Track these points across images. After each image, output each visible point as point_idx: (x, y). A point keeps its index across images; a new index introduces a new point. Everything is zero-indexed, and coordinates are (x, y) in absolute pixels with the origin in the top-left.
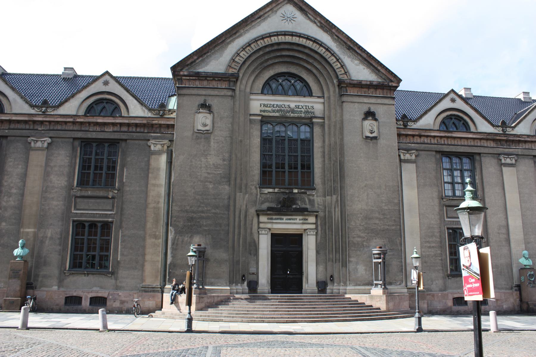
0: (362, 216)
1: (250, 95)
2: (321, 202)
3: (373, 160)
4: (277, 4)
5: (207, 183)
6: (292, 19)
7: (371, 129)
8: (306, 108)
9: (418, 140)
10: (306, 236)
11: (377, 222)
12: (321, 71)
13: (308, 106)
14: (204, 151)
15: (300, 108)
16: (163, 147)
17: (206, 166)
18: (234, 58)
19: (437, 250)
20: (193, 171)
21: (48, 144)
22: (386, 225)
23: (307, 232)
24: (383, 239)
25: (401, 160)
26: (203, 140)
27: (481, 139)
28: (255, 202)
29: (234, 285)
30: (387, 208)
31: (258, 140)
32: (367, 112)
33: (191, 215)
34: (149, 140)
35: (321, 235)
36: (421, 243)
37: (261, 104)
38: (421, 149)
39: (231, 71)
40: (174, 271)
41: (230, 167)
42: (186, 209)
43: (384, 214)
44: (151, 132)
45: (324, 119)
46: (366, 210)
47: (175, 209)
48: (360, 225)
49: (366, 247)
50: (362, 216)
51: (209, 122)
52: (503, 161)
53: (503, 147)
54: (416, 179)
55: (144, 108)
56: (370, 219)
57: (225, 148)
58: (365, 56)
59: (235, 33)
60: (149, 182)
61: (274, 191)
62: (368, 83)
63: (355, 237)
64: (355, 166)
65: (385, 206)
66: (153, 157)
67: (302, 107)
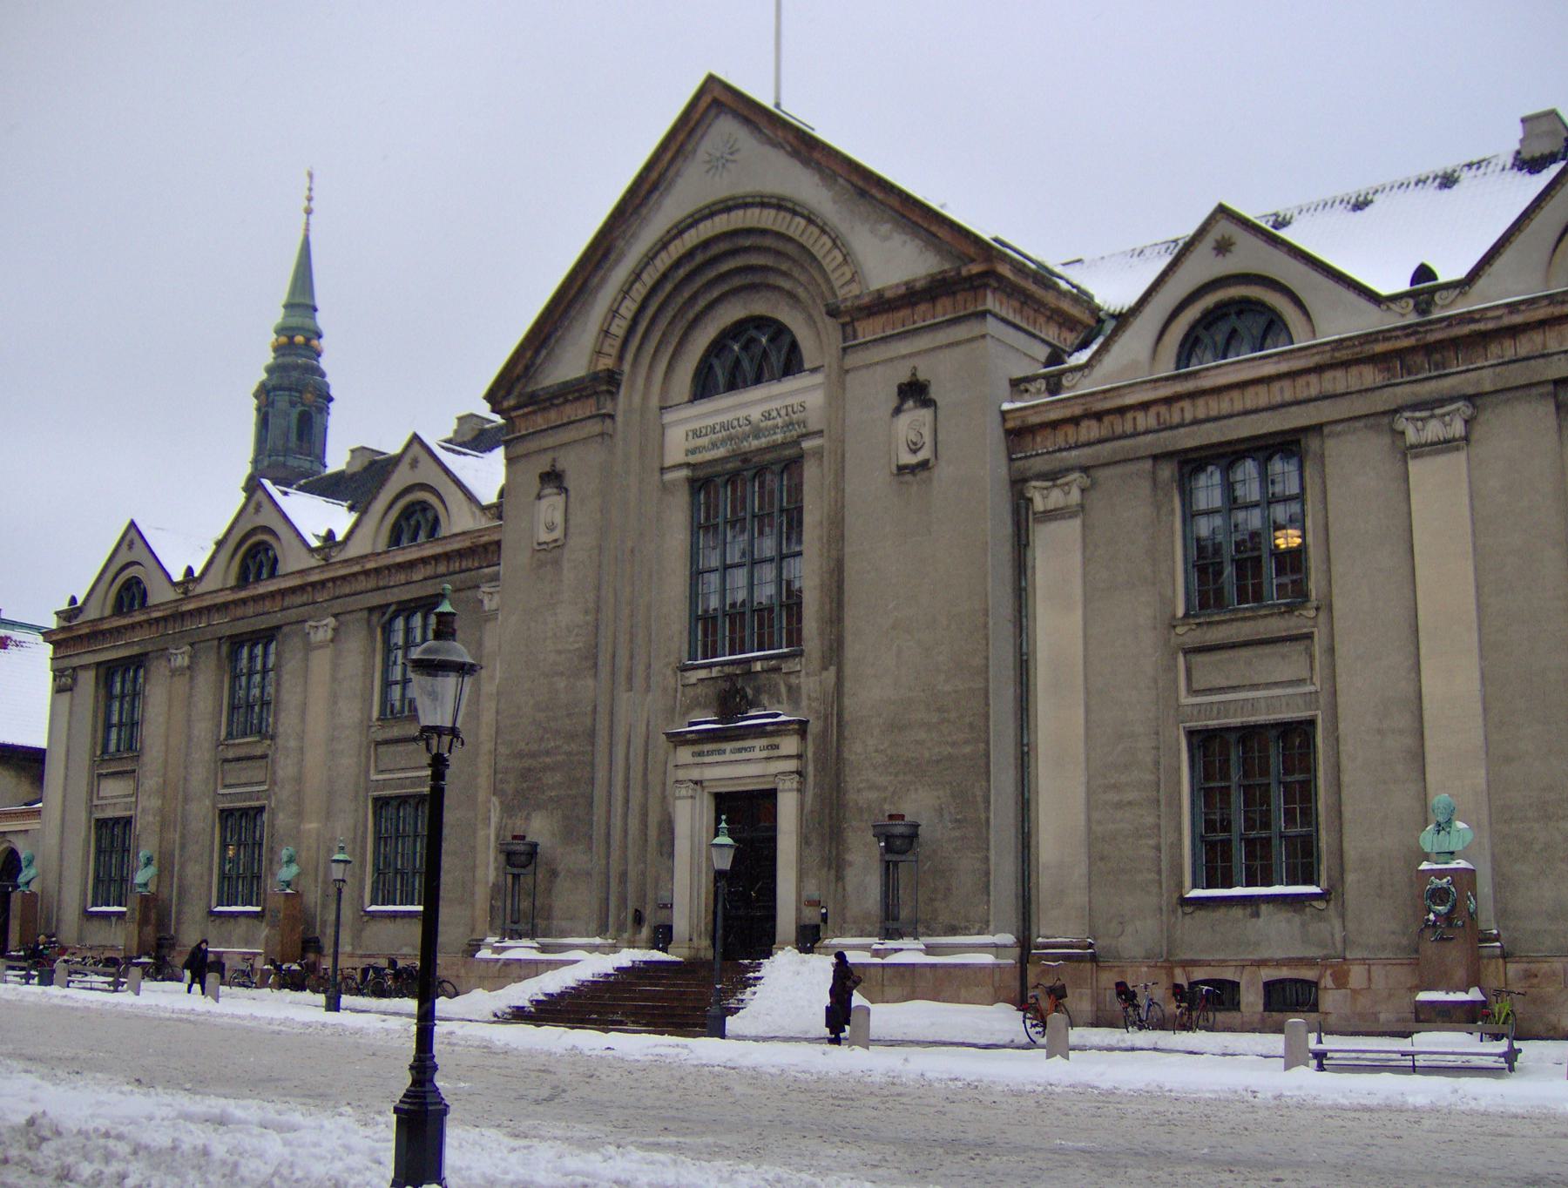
11: (922, 735)
14: (551, 595)
15: (774, 418)
21: (334, 629)
27: (1319, 369)
33: (528, 763)
34: (478, 587)
36: (1090, 793)
38: (1102, 461)
48: (876, 751)
51: (558, 518)
52: (1412, 436)
53: (1413, 378)
54: (1079, 571)
55: (474, 509)
61: (709, 676)
67: (779, 414)
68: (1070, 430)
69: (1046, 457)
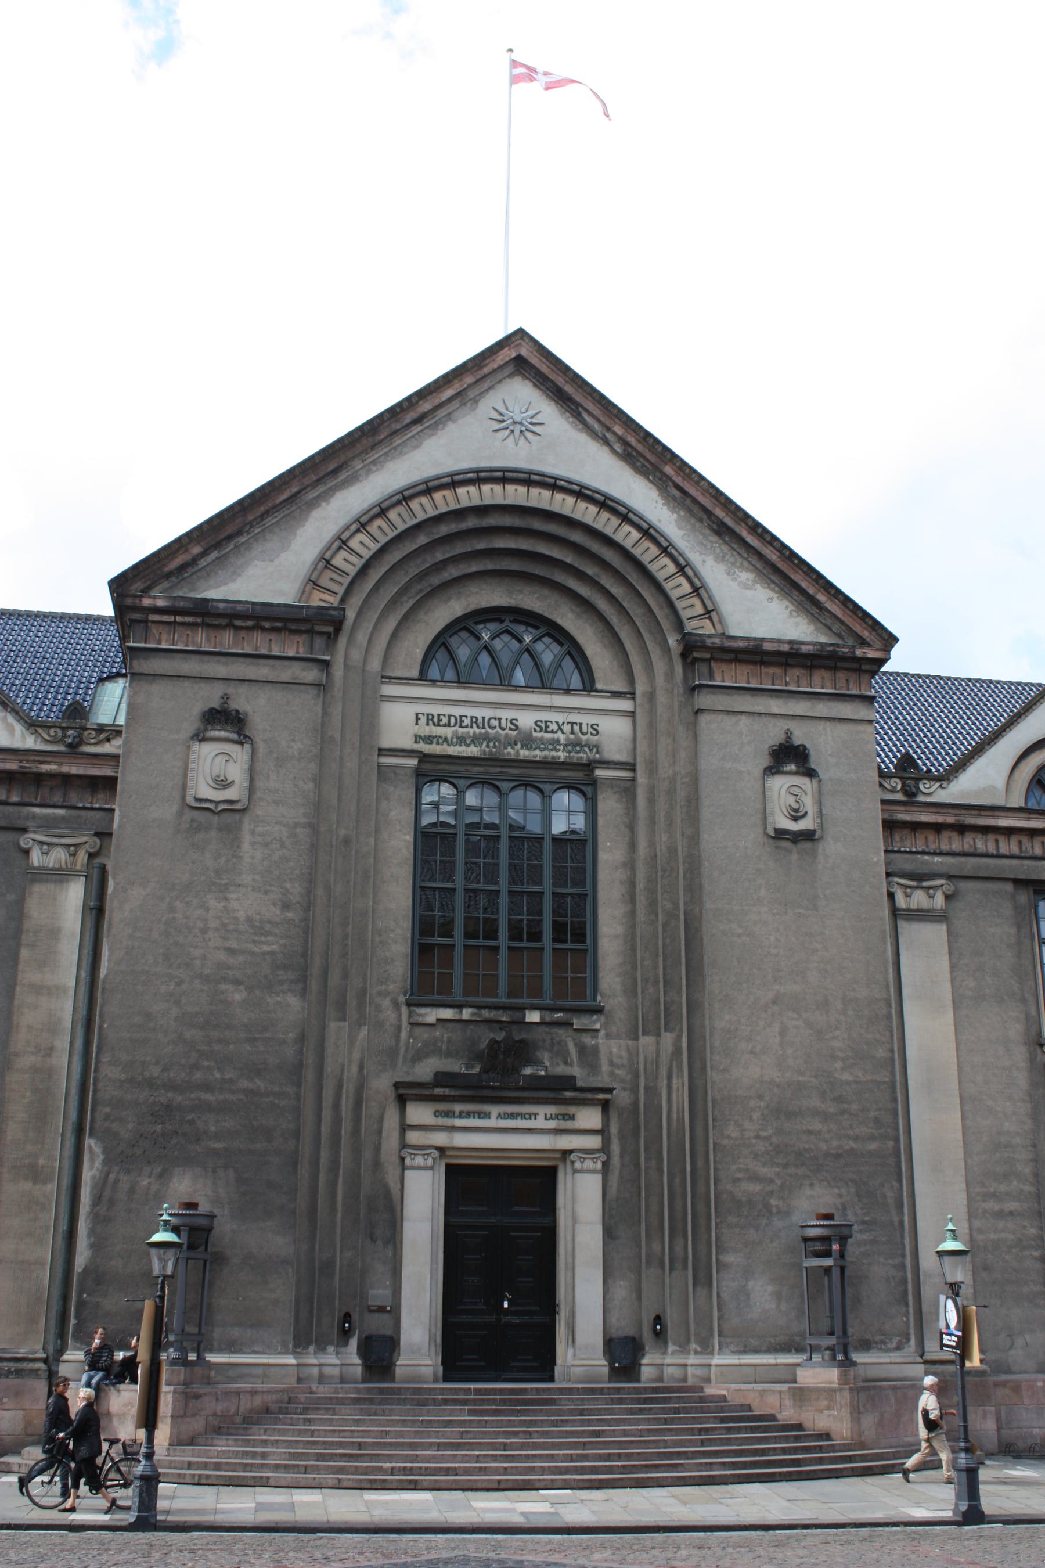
0: (763, 1104)
1: (382, 682)
2: (621, 1057)
3: (802, 911)
4: (478, 377)
5: (223, 987)
6: (527, 429)
7: (795, 806)
8: (572, 732)
9: (956, 843)
10: (569, 1177)
11: (817, 1125)
12: (625, 604)
13: (581, 724)
14: (217, 872)
15: (552, 732)
16: (73, 855)
17: (224, 925)
18: (327, 556)
19: (1026, 1224)
20: (176, 943)
22: (848, 1136)
23: (573, 1162)
24: (839, 1188)
25: (896, 913)
26: (213, 834)
28: (392, 1053)
29: (312, 1349)
30: (851, 1078)
31: (407, 837)
32: (781, 744)
33: (164, 1097)
34: (24, 830)
35: (621, 1172)
36: (970, 1199)
37: (417, 714)
38: (965, 873)
39: (317, 599)
40: (98, 1299)
41: (307, 930)
42: (147, 1074)
43: (839, 1099)
44: (34, 801)
45: (634, 770)
46: (778, 1086)
47: (110, 1075)
48: (758, 1137)
49: (778, 1213)
50: (763, 1104)
51: (236, 772)
54: (948, 976)
55: (11, 719)
56: (790, 1115)
57: (292, 864)
58: (773, 556)
59: (335, 472)
60: (20, 978)
61: (457, 1017)
62: (785, 648)
63: (739, 1180)
64: (740, 931)
65: (843, 1069)
66: (37, 888)
67: (560, 729)
68: (931, 837)
69: (907, 856)
